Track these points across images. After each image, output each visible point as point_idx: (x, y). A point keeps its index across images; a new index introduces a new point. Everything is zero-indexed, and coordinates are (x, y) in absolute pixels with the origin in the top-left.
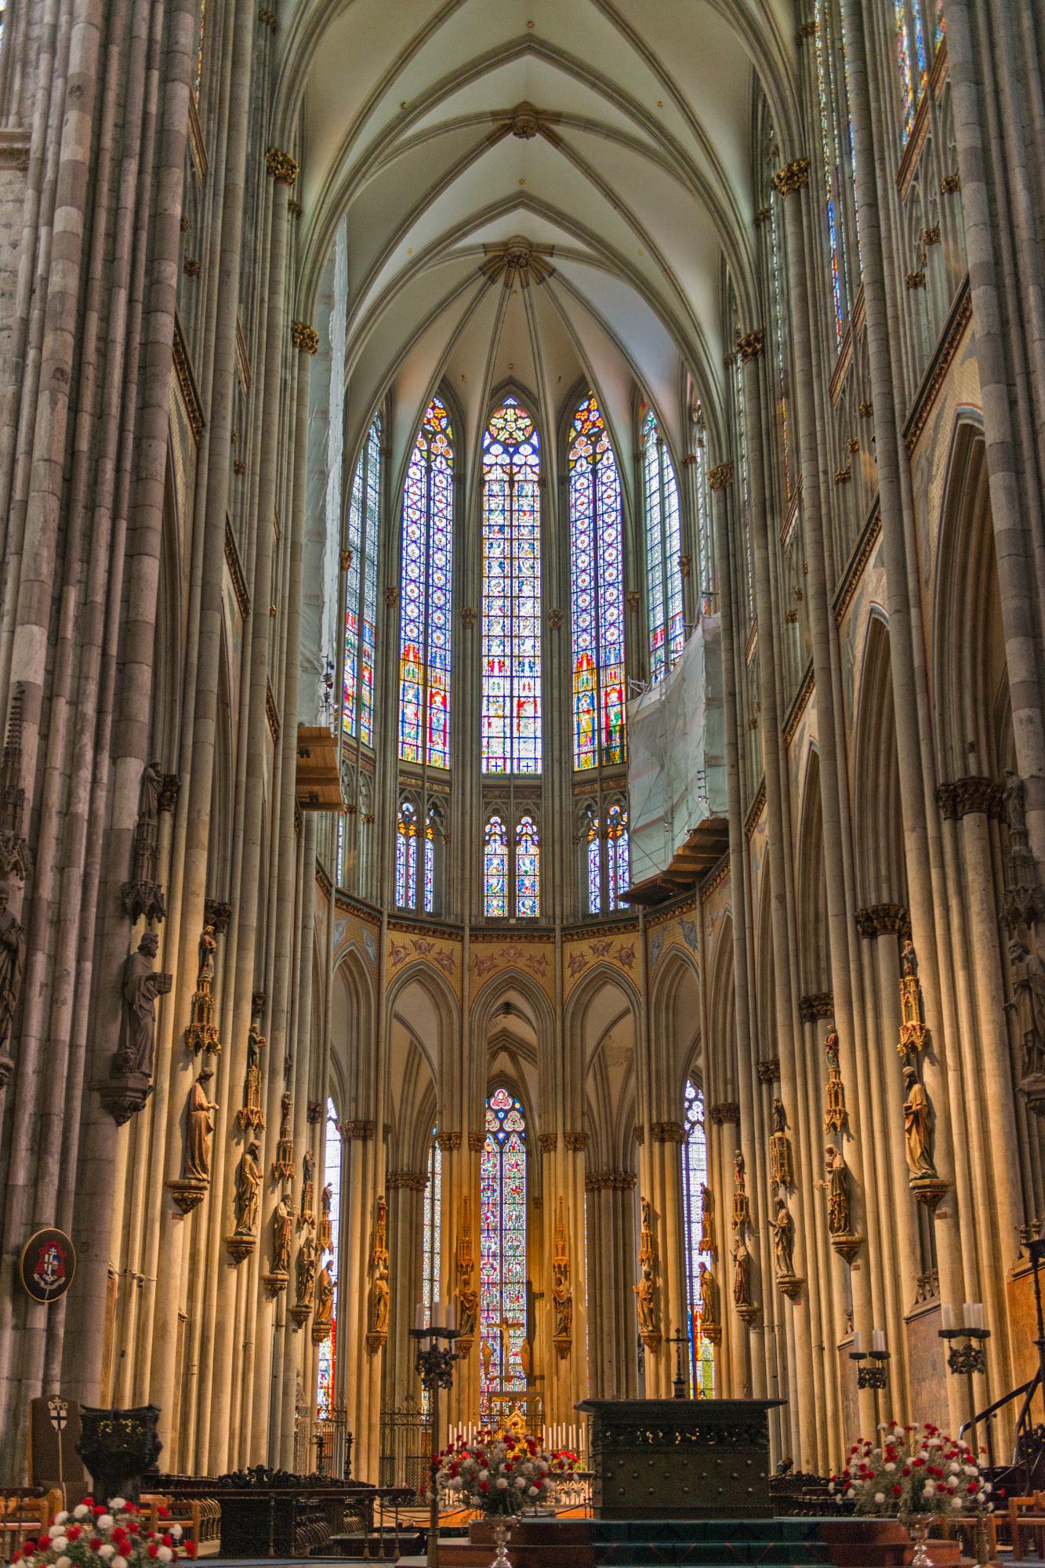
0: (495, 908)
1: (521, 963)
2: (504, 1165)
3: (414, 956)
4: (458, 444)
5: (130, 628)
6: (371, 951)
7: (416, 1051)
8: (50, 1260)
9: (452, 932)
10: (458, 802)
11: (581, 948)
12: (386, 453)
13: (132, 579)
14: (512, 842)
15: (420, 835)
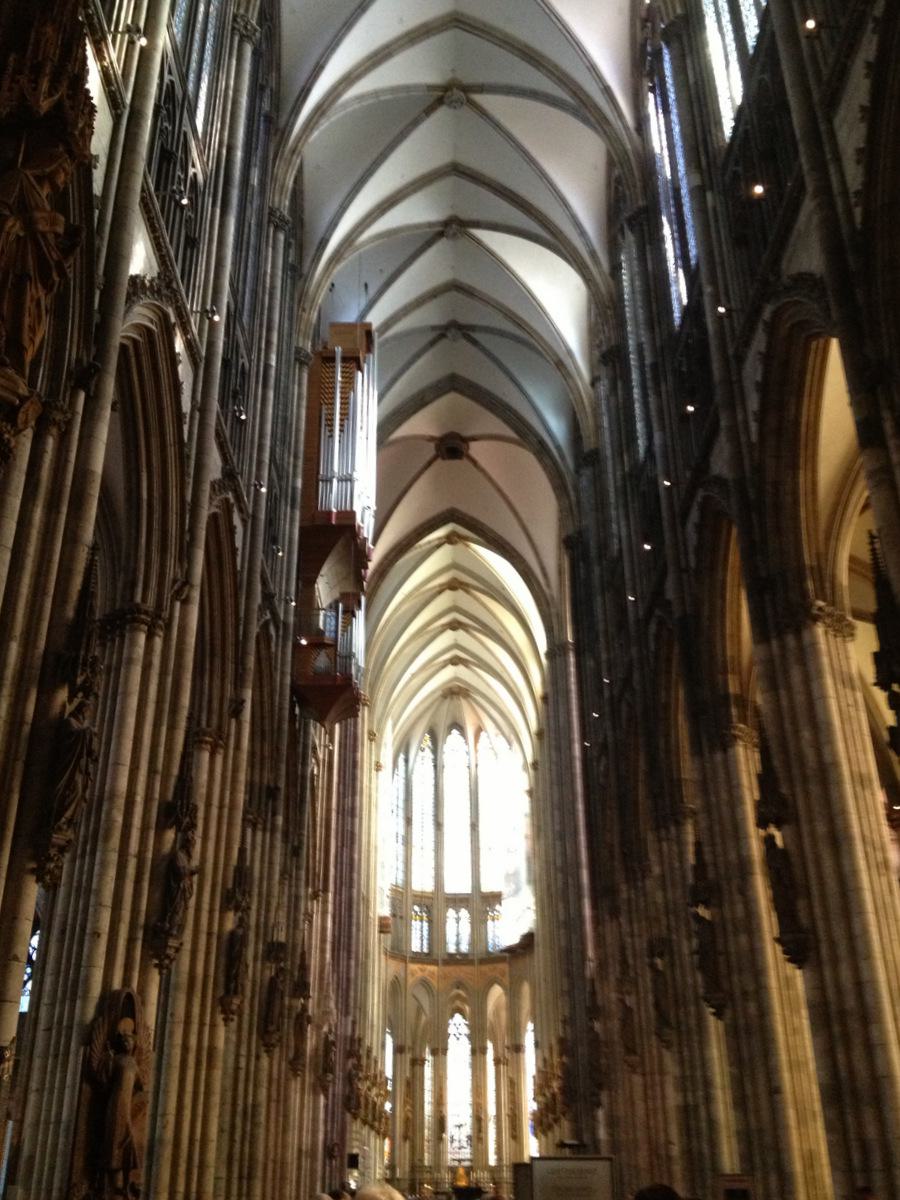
0: (452, 949)
1: (462, 974)
2: (459, 1049)
3: (419, 974)
4: (435, 751)
5: (348, 980)
6: (403, 974)
7: (419, 1010)
8: (336, 1149)
9: (435, 962)
10: (434, 905)
11: (485, 968)
12: (406, 761)
13: (348, 966)
14: (458, 920)
15: (421, 921)
